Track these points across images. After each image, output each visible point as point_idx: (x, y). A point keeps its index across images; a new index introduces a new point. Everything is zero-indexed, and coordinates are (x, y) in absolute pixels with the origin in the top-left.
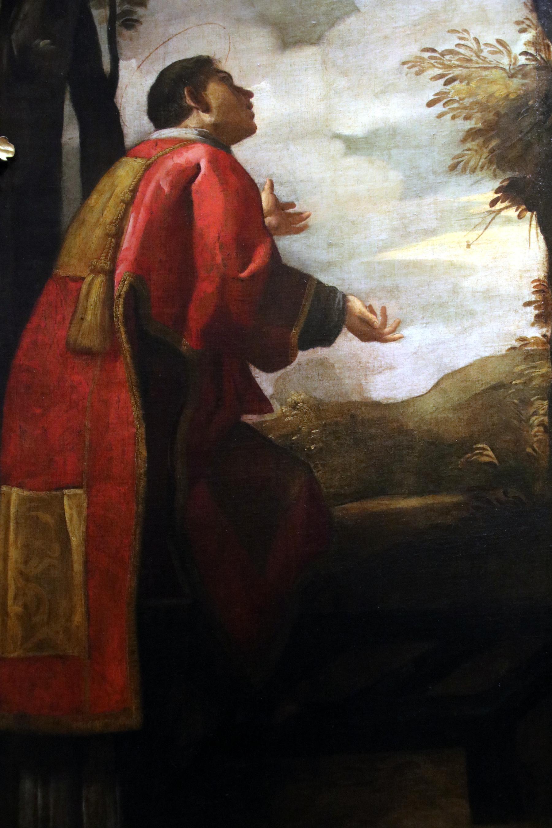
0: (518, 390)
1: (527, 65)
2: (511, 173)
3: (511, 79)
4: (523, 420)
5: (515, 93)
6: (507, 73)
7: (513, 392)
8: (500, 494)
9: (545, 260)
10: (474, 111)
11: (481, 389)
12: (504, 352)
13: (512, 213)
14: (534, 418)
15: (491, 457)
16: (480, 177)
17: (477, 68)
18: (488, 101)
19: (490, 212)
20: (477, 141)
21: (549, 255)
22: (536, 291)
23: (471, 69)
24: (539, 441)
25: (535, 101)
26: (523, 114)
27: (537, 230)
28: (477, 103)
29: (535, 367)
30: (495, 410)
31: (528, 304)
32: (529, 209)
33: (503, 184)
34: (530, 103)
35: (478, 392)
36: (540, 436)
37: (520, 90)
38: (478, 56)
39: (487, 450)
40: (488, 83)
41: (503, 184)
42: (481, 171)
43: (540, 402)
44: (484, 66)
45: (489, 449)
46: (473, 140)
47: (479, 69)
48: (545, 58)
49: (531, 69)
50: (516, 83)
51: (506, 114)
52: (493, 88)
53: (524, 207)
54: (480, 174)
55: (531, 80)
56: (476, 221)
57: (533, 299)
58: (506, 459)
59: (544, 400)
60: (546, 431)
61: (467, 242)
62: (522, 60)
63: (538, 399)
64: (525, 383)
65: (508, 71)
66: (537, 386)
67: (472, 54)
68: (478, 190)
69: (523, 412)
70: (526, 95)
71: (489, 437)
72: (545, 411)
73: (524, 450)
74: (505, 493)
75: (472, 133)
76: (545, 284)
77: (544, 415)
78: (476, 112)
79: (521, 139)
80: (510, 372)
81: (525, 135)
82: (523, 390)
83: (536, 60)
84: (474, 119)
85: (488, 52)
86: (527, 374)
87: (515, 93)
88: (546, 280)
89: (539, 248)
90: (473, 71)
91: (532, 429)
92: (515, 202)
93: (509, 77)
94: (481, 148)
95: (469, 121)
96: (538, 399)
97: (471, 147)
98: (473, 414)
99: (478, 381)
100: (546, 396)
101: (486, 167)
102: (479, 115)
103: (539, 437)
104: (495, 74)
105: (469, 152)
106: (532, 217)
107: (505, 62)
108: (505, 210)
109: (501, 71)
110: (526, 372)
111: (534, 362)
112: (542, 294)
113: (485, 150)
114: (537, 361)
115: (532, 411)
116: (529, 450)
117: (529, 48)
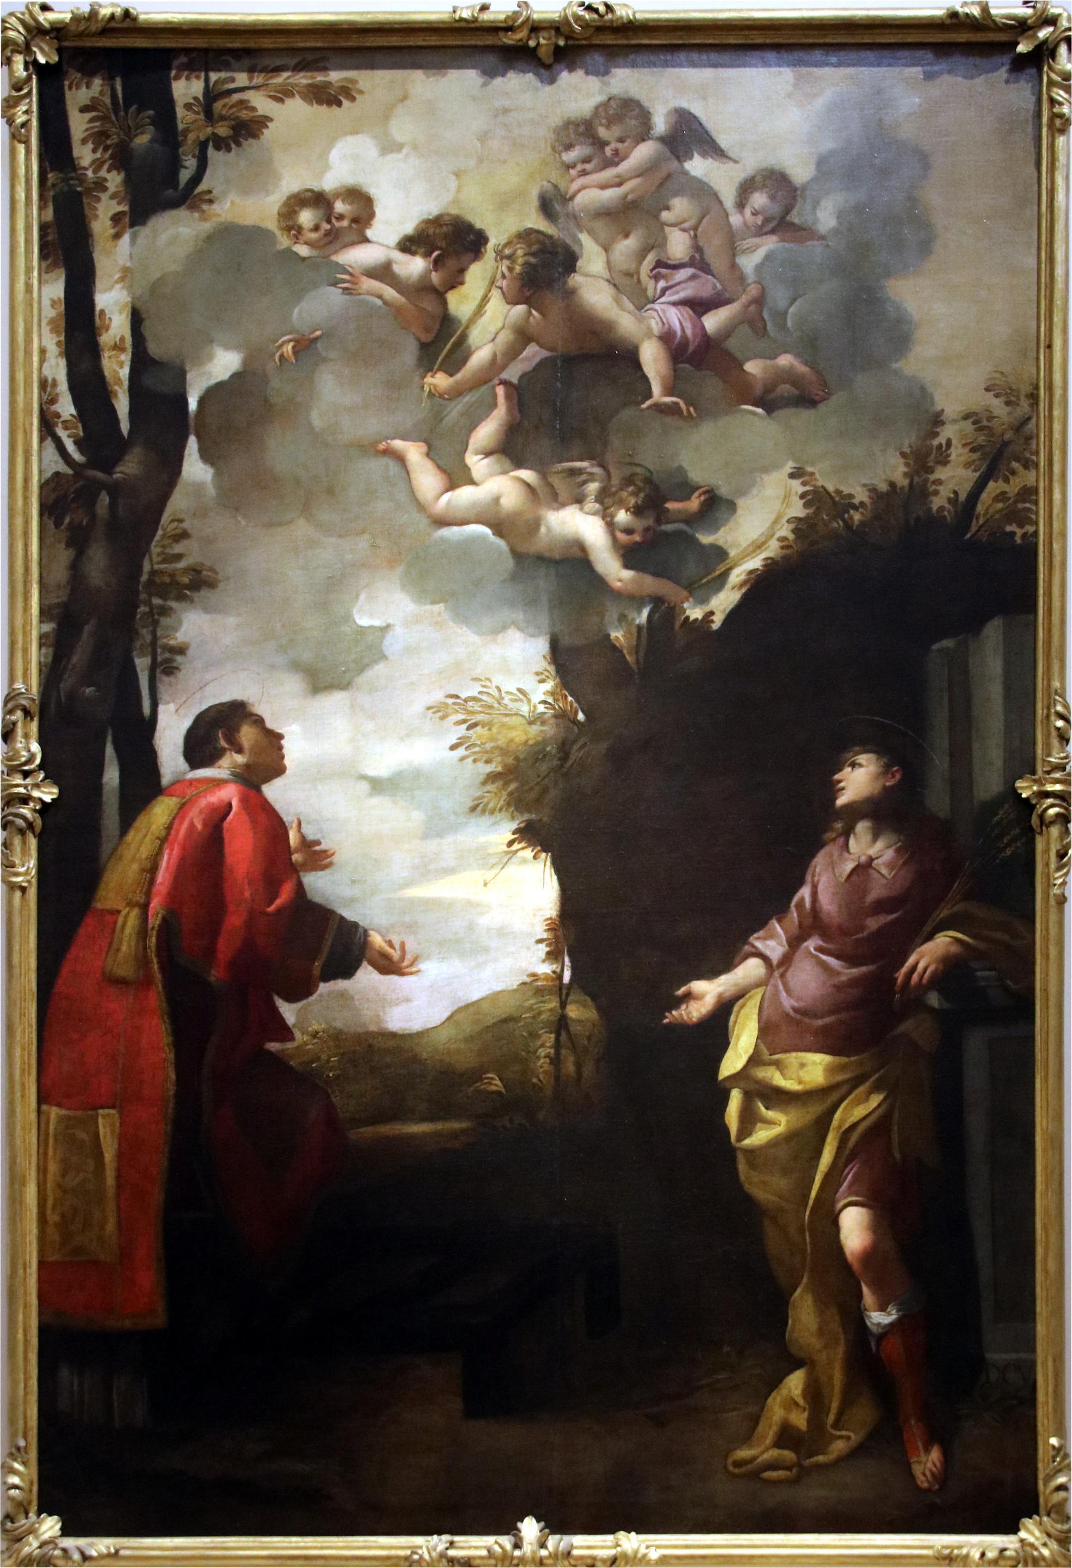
12: (515, 987)
13: (528, 853)
14: (540, 1050)
19: (507, 853)
28: (498, 747)
29: (542, 1002)
30: (505, 1041)
32: (545, 850)
34: (548, 749)
36: (547, 1067)
38: (499, 704)
43: (547, 1035)
46: (493, 783)
50: (535, 729)
51: (525, 759)
52: (513, 734)
54: (498, 816)
56: (494, 861)
60: (551, 1063)
62: (541, 708)
64: (534, 1017)
70: (544, 742)
73: (530, 1080)
74: (511, 1120)
77: (550, 1047)
79: (538, 783)
92: (531, 843)
102: (499, 759)
104: (516, 720)
107: (525, 709)
115: (540, 1043)
116: (535, 1080)
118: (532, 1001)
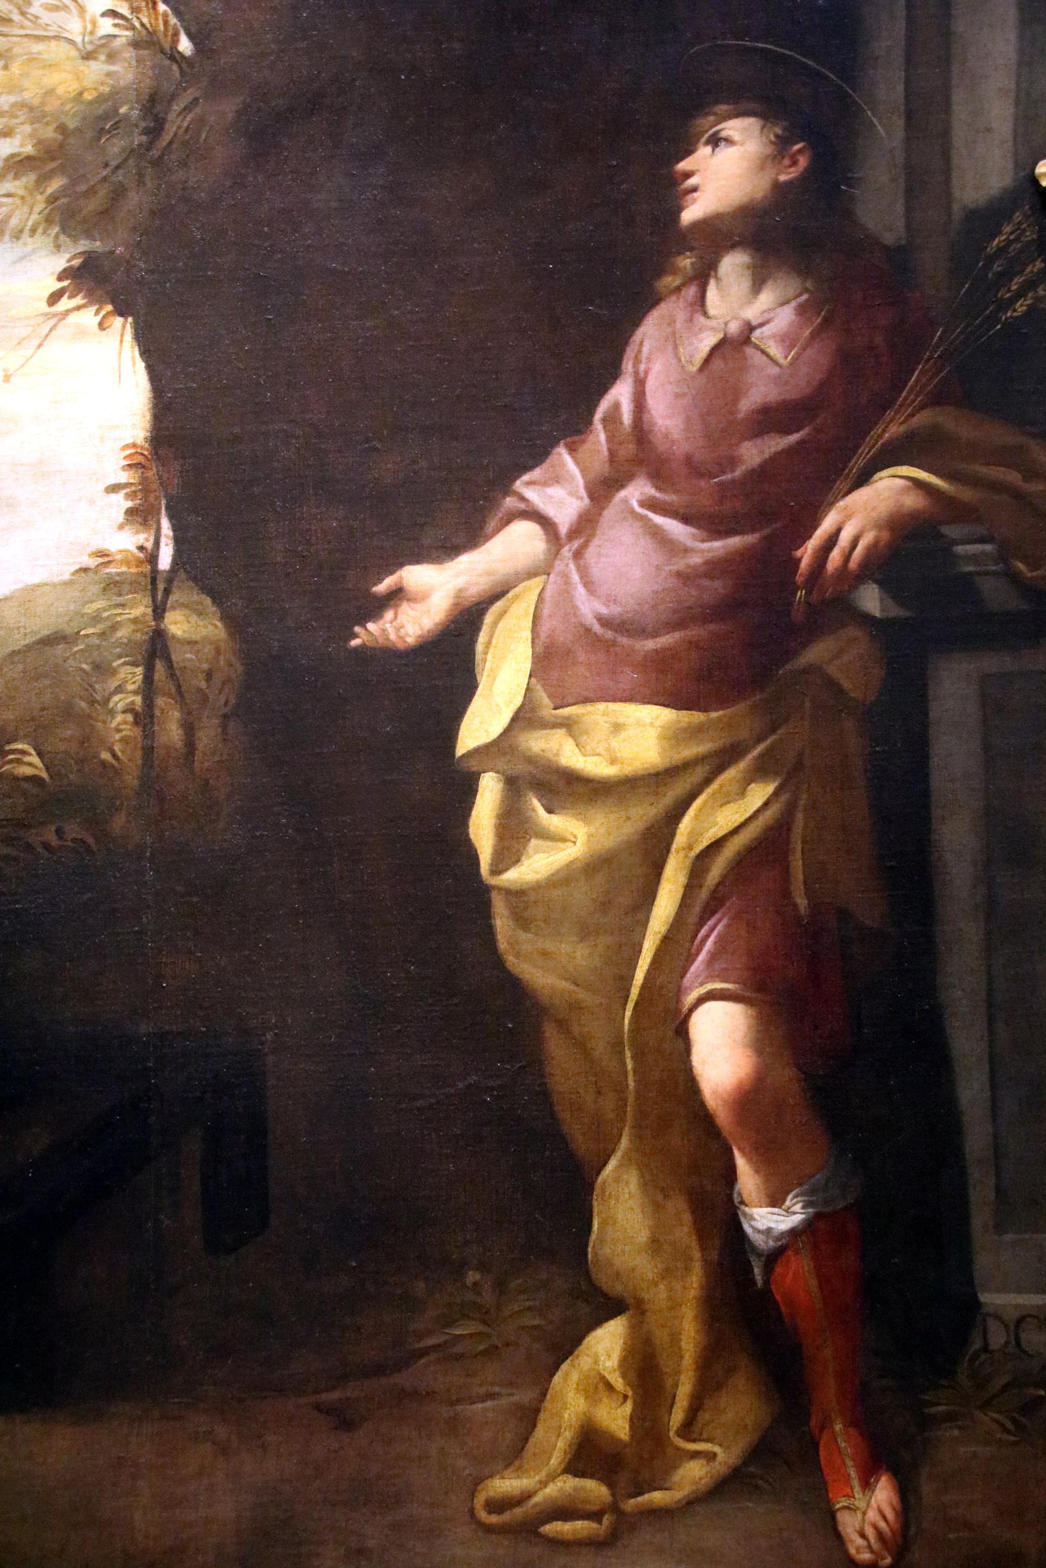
0: (89, 647)
1: (115, 36)
2: (87, 242)
3: (87, 63)
4: (97, 701)
5: (95, 89)
6: (79, 50)
7: (81, 650)
8: (49, 835)
9: (146, 408)
10: (17, 121)
11: (23, 643)
12: (67, 577)
13: (89, 317)
14: (116, 698)
15: (36, 767)
16: (30, 248)
17: (21, 36)
18: (43, 103)
19: (48, 316)
20: (24, 179)
21: (155, 398)
22: (129, 465)
23: (10, 38)
24: (124, 740)
25: (132, 109)
26: (109, 132)
27: (133, 352)
28: (23, 105)
29: (122, 605)
30: (47, 682)
31: (114, 489)
32: (121, 311)
33: (73, 263)
34: (123, 110)
35: (17, 648)
36: (128, 731)
37: (102, 84)
38: (23, 14)
39: (30, 755)
40: (44, 67)
41: (73, 263)
42: (31, 236)
43: (129, 669)
44: (36, 33)
45: (33, 752)
46: (16, 177)
47: (26, 40)
48: (148, 26)
49: (122, 45)
50: (96, 70)
51: (78, 130)
52: (53, 78)
53: (109, 308)
54: (29, 243)
55: (123, 67)
56: (21, 331)
57: (123, 480)
58: (63, 772)
59: (137, 666)
60: (136, 723)
61: (4, 370)
62: (107, 26)
63: (125, 664)
64: (103, 635)
65: (80, 46)
66: (126, 641)
67: (11, 7)
68: (26, 273)
69: (97, 686)
70: (114, 96)
71: (35, 731)
72: (137, 684)
73: (96, 756)
74: (59, 832)
75: (15, 163)
76: (146, 453)
77: (135, 693)
78: (22, 124)
79: (105, 179)
80: (76, 613)
81: (114, 172)
82: (99, 647)
83: (133, 28)
84: (18, 136)
85: (41, 6)
86: (108, 618)
87: (95, 89)
88: (147, 445)
89: (137, 385)
90: (15, 43)
91: (113, 718)
92: (94, 298)
93: (83, 58)
94: (31, 194)
95: (8, 140)
96: (125, 664)
97: (13, 191)
98: (7, 688)
99: (18, 628)
100: (139, 657)
101: (40, 230)
102: (27, 129)
103: (124, 733)
104: (56, 51)
105: (10, 200)
106: (124, 327)
107: (74, 27)
108: (76, 313)
109: (68, 46)
110: (106, 614)
111: (120, 595)
112: (140, 471)
113: (39, 197)
114: (127, 594)
115: (113, 684)
116: (105, 756)
117: (118, 3)
118: (100, 604)
